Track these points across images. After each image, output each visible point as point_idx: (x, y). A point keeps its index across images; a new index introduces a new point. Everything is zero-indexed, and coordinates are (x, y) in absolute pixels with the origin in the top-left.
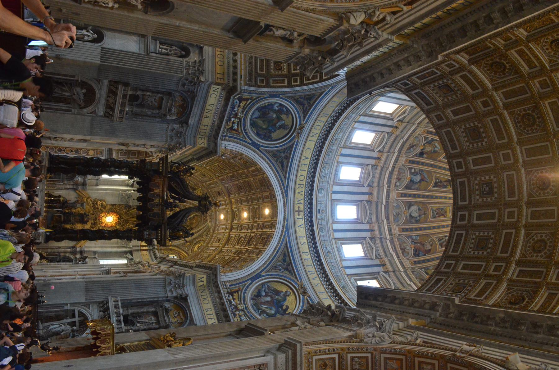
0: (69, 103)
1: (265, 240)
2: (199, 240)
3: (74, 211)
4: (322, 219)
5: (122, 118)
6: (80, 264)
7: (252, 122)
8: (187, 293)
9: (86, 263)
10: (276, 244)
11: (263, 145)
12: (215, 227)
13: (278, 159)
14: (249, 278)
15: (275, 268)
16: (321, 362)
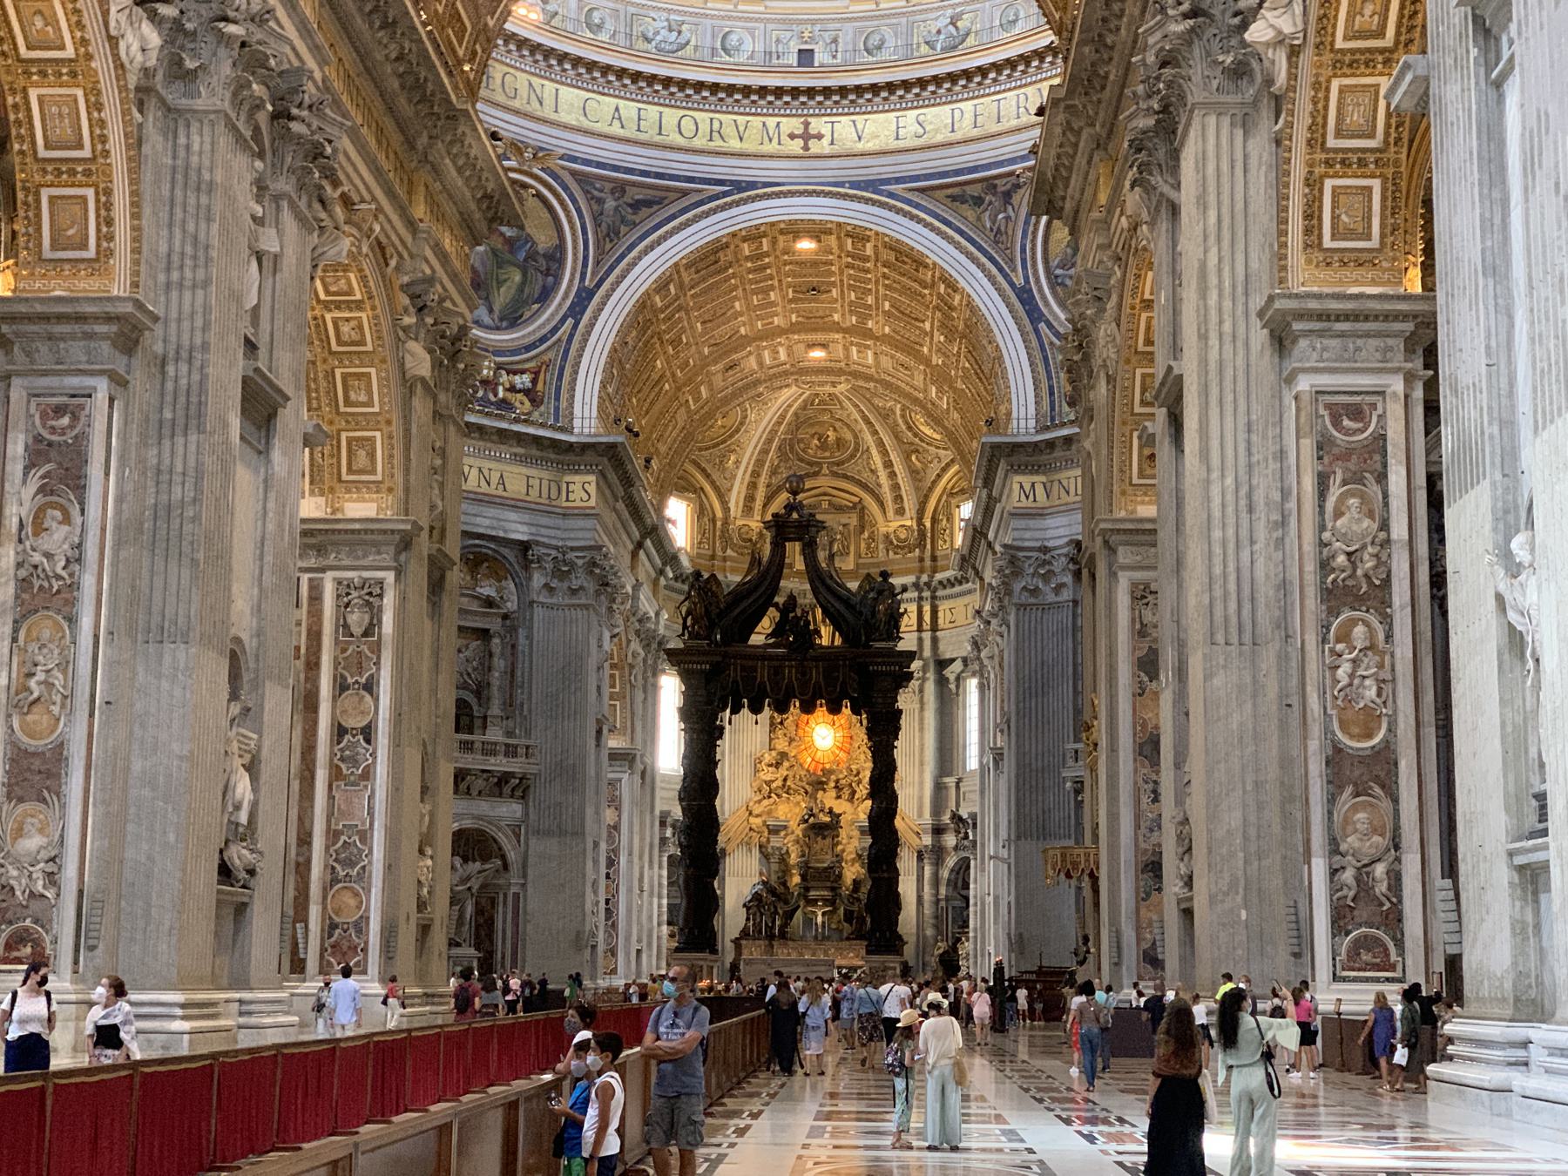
0: (493, 902)
1: (905, 259)
2: (900, 421)
3: (794, 859)
4: (835, 41)
5: (527, 747)
6: (975, 835)
7: (504, 324)
8: (1066, 540)
9: (973, 816)
10: (919, 228)
11: (578, 276)
12: (856, 375)
13: (623, 221)
14: (1029, 328)
15: (998, 236)
16: (1145, 466)
